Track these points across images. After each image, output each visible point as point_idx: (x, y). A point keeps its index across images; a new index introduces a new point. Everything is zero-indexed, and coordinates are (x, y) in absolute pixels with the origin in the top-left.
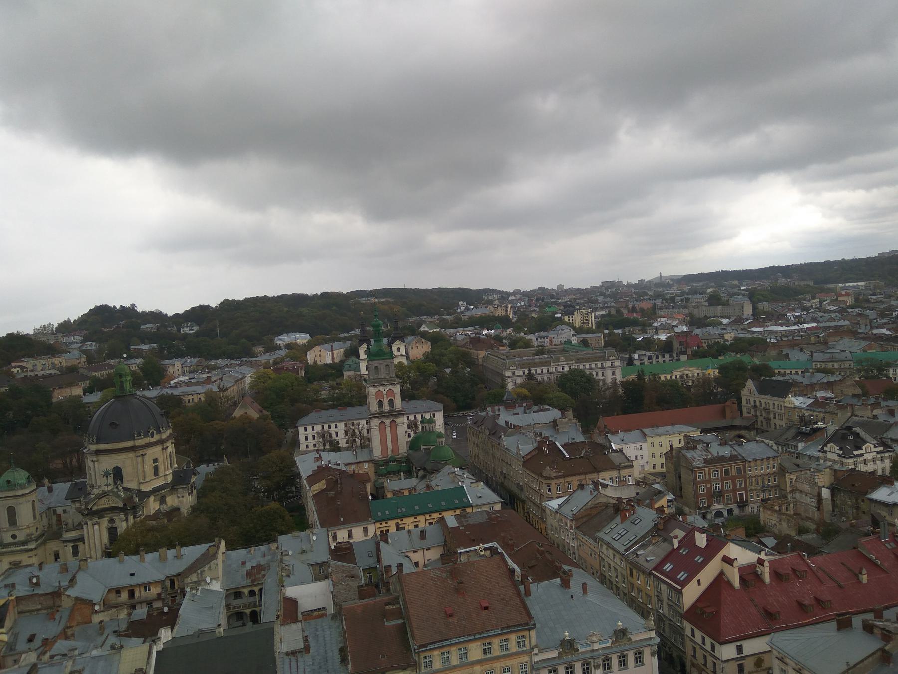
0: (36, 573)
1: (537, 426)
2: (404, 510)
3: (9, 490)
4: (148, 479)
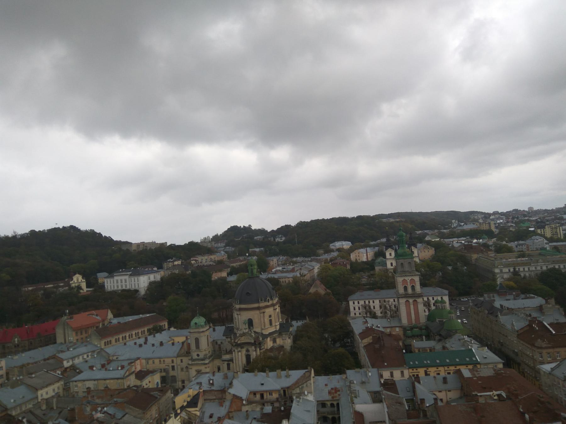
0: (212, 378)
1: (526, 309)
2: (429, 362)
3: (195, 328)
4: (266, 327)
